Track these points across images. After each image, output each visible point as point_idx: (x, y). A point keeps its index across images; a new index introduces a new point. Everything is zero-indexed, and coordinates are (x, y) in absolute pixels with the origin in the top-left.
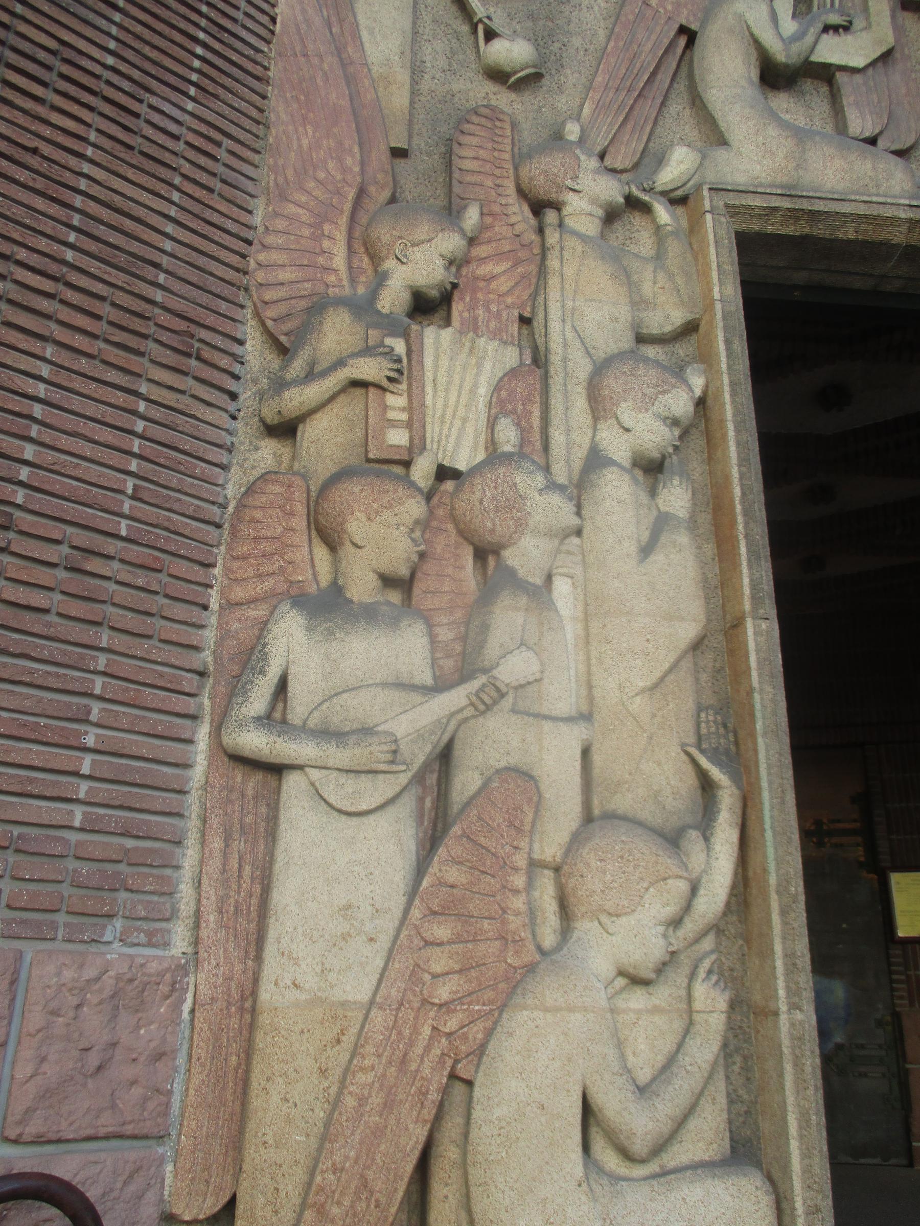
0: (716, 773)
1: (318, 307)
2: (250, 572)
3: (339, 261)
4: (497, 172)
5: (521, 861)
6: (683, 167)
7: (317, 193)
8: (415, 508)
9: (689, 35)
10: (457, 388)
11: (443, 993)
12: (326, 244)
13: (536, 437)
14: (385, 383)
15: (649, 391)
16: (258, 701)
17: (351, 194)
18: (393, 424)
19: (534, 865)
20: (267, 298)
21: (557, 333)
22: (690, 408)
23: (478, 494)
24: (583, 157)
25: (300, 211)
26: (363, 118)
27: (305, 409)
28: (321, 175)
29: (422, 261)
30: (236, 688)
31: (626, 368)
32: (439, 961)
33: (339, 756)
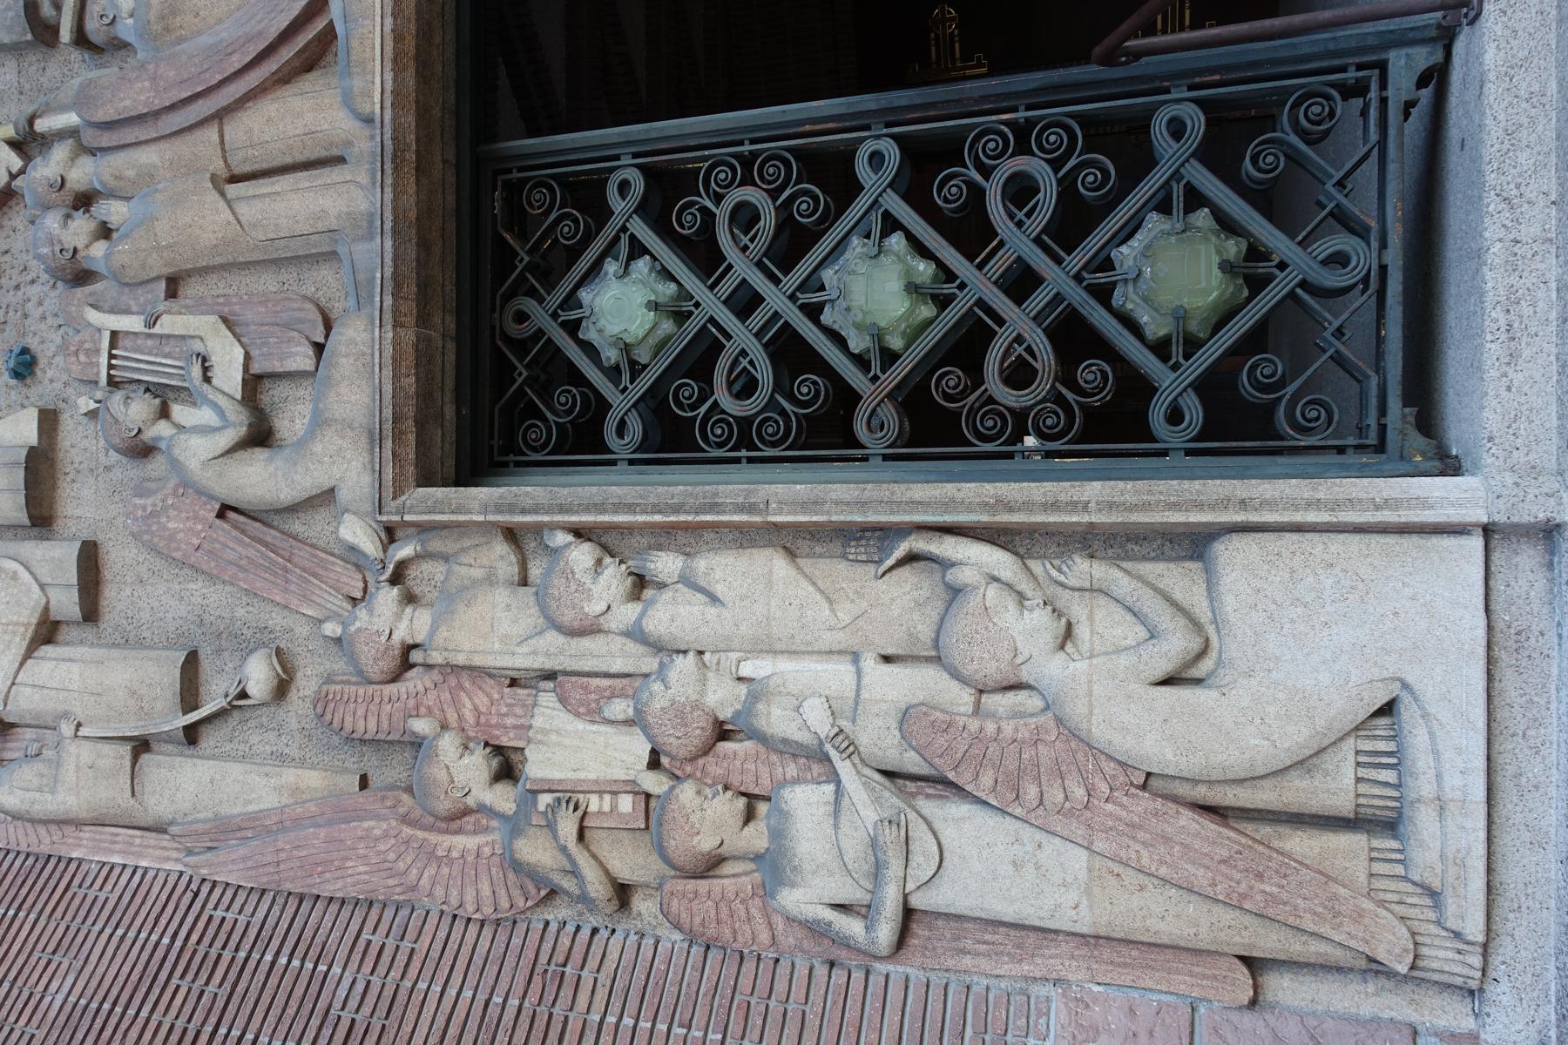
0: (900, 551)
1: (517, 866)
2: (747, 927)
3: (469, 842)
4: (377, 700)
5: (974, 725)
6: (359, 532)
7: (409, 860)
8: (687, 792)
9: (224, 511)
10: (578, 751)
11: (1079, 793)
12: (455, 854)
13: (618, 683)
14: (579, 813)
15: (573, 587)
16: (853, 927)
17: (408, 831)
18: (614, 807)
19: (977, 709)
20: (507, 905)
21: (523, 659)
22: (587, 546)
23: (672, 740)
24: (358, 624)
25: (426, 874)
26: (336, 813)
27: (605, 880)
28: (392, 856)
29: (467, 771)
30: (846, 943)
31: (554, 605)
32: (1055, 796)
33: (894, 869)
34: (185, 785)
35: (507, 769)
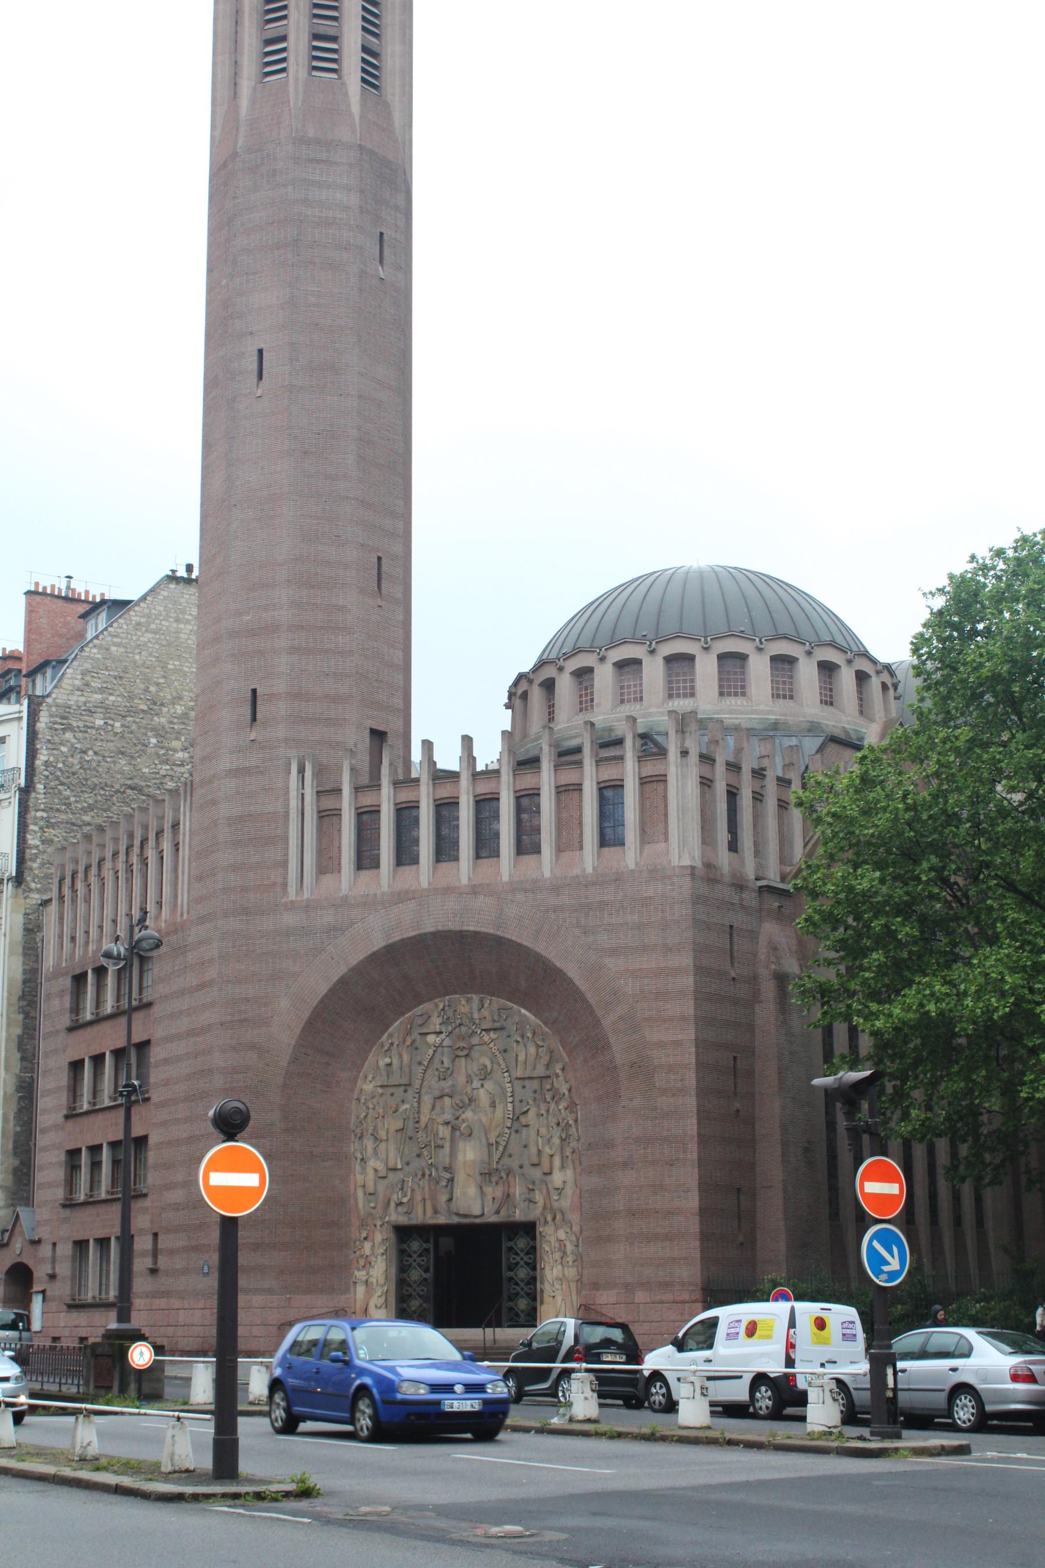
29: (364, 1235)
34: (360, 1193)
35: (365, 1239)
